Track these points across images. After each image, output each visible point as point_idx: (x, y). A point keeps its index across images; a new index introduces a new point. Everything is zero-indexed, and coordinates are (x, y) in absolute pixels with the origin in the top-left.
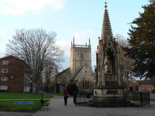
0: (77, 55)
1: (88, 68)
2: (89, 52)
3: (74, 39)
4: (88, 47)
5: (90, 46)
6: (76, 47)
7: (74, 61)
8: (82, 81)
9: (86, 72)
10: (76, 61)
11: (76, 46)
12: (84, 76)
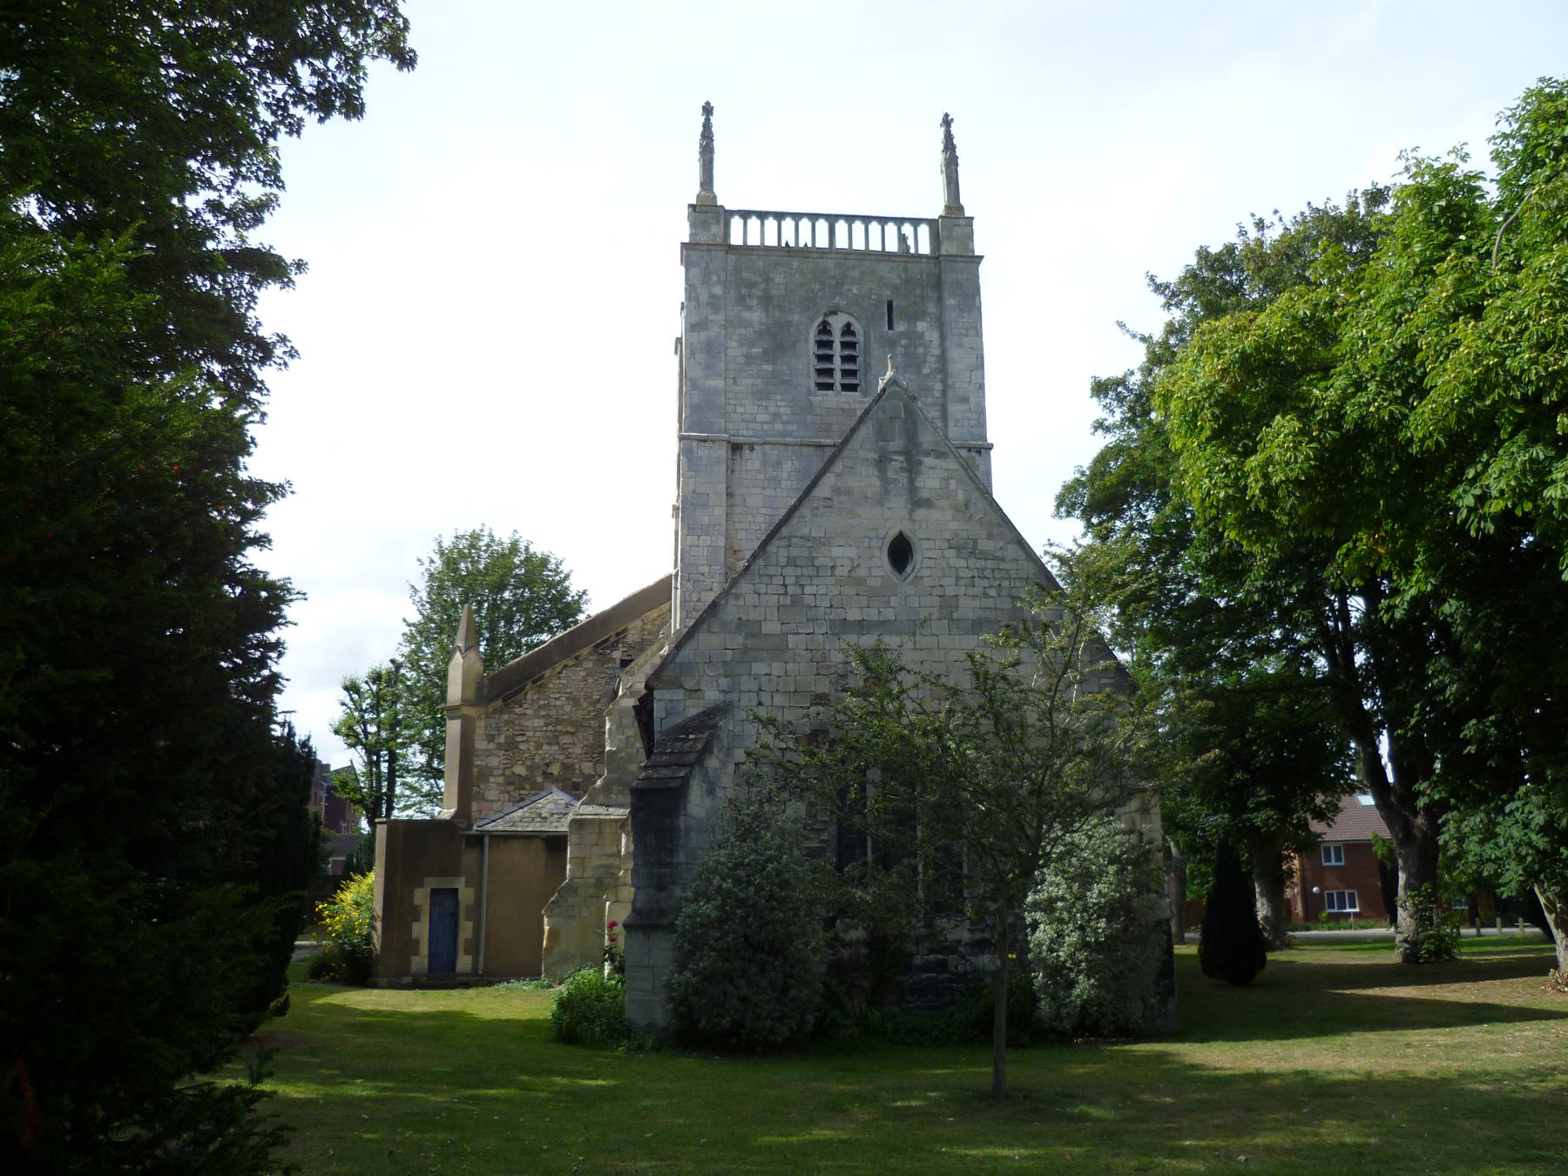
0: (749, 359)
1: (929, 482)
2: (951, 315)
3: (707, 126)
4: (935, 238)
5: (953, 224)
6: (736, 239)
7: (702, 451)
8: (816, 736)
9: (900, 552)
10: (736, 448)
11: (736, 223)
12: (862, 626)
